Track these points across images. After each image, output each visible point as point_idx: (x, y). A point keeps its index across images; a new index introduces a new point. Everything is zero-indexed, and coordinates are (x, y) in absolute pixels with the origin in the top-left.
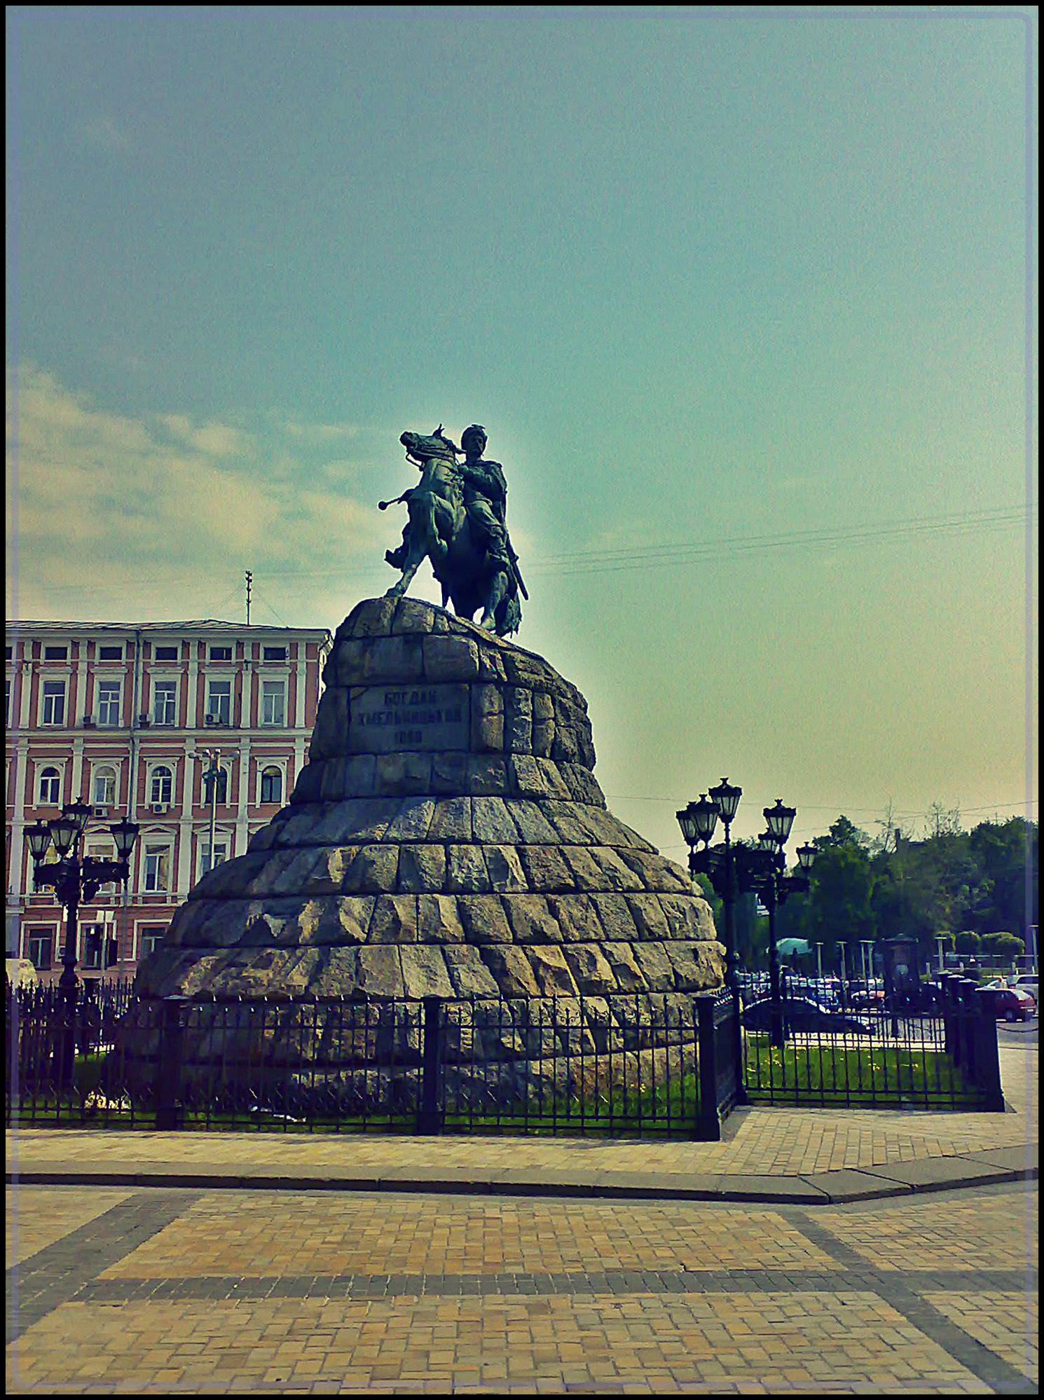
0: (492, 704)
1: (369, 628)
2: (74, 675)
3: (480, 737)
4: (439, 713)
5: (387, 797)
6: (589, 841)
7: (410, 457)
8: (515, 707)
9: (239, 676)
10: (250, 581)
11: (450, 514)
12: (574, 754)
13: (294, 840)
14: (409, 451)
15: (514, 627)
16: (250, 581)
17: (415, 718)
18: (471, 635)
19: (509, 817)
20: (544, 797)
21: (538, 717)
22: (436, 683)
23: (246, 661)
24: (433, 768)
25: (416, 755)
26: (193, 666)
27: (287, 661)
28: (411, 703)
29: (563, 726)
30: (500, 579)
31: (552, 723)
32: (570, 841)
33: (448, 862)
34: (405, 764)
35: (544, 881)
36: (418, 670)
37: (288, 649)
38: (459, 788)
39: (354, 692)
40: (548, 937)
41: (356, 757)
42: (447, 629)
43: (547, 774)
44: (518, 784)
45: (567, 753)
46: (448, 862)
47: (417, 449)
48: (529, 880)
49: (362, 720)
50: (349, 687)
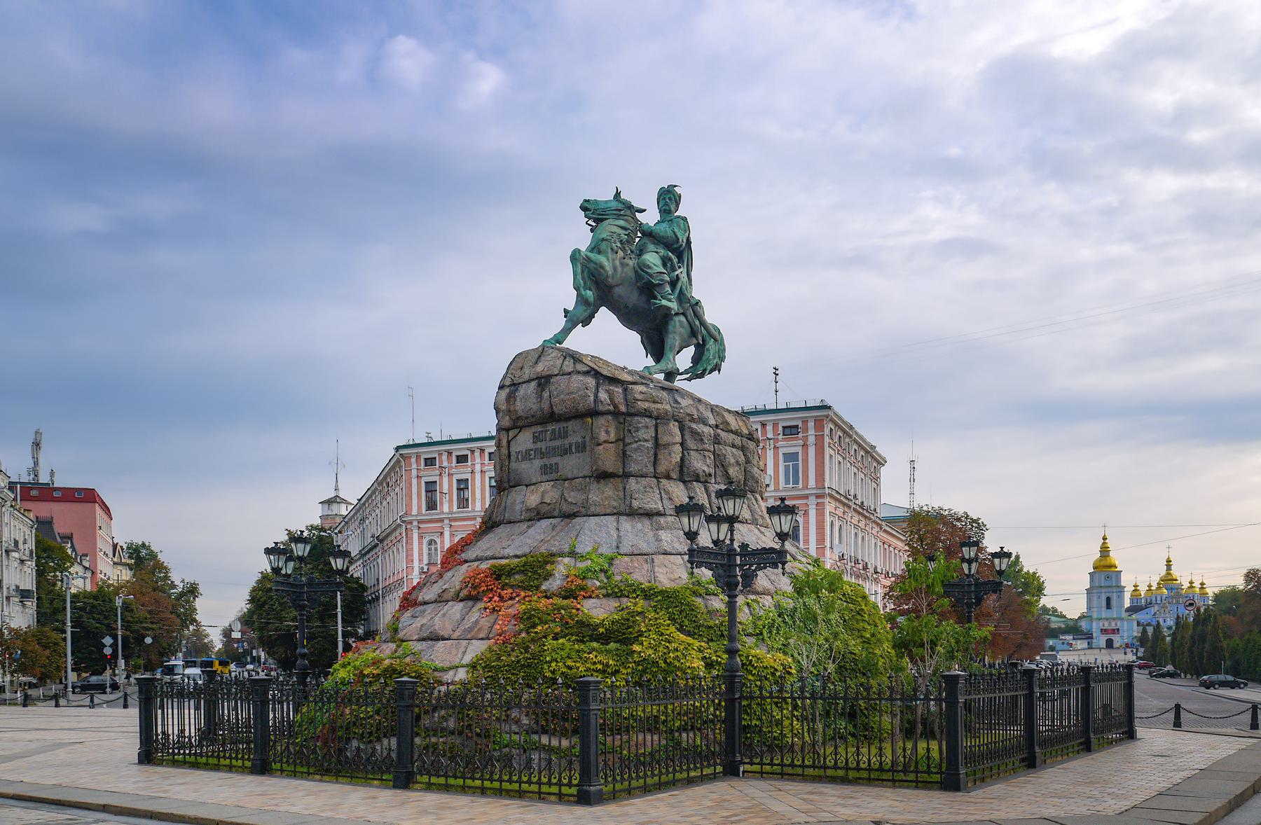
0: (607, 432)
3: (596, 462)
4: (570, 446)
5: (530, 520)
8: (634, 434)
17: (552, 452)
18: (593, 372)
20: (659, 514)
21: (660, 442)
22: (568, 419)
24: (563, 494)
25: (552, 483)
27: (800, 435)
29: (697, 450)
30: (678, 324)
31: (678, 448)
32: (666, 550)
36: (546, 406)
39: (511, 434)
41: (514, 489)
42: (571, 369)
43: (667, 492)
45: (698, 475)
49: (518, 458)
50: (507, 430)
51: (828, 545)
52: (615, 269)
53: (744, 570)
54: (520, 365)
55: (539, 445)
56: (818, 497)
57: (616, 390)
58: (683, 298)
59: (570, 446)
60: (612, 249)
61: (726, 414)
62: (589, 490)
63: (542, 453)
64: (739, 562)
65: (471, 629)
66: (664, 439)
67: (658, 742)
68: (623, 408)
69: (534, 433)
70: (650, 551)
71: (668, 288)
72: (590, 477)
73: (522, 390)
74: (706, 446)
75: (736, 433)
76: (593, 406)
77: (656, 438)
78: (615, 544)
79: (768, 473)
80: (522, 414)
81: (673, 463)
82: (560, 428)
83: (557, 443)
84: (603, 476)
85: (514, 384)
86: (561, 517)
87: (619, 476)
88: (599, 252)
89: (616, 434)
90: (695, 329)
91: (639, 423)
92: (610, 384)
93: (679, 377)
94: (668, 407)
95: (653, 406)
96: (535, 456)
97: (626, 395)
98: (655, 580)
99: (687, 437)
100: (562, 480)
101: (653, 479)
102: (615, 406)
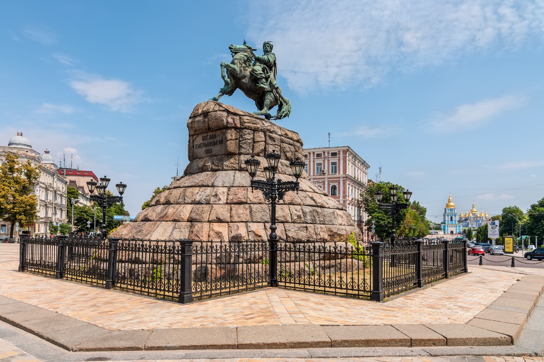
0: (231, 135)
4: (217, 141)
9: (324, 160)
17: (210, 144)
21: (255, 140)
23: (326, 157)
24: (213, 162)
26: (312, 159)
27: (337, 156)
29: (272, 145)
33: (198, 193)
34: (205, 161)
35: (232, 200)
37: (337, 152)
38: (220, 168)
40: (222, 220)
48: (227, 199)
51: (348, 195)
52: (241, 71)
56: (343, 178)
57: (236, 118)
58: (271, 84)
59: (217, 141)
60: (240, 63)
61: (286, 131)
65: (163, 217)
66: (257, 139)
67: (242, 270)
68: (239, 125)
71: (264, 80)
72: (224, 155)
74: (276, 143)
75: (291, 139)
76: (225, 124)
77: (254, 139)
78: (232, 182)
79: (326, 169)
81: (261, 149)
88: (234, 64)
89: (235, 136)
90: (277, 98)
91: (246, 132)
93: (271, 119)
94: (259, 126)
95: (252, 125)
97: (240, 120)
98: (247, 198)
99: (268, 139)
102: (235, 125)
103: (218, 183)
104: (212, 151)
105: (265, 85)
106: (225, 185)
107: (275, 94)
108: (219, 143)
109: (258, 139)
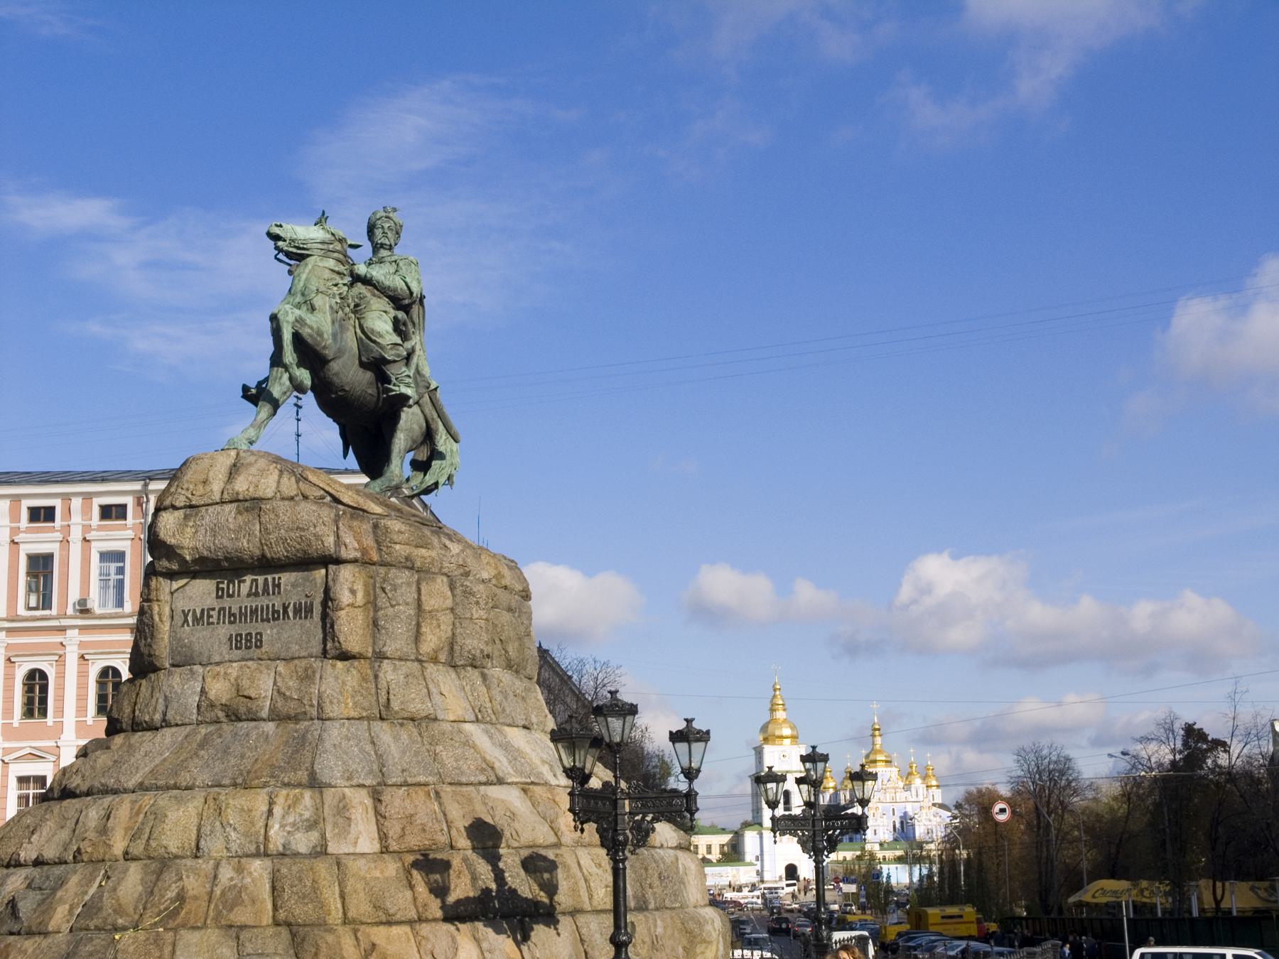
0: (353, 592)
1: (193, 494)
2: (65, 542)
4: (285, 608)
6: (483, 779)
7: (281, 256)
8: (390, 595)
10: (300, 407)
11: (320, 334)
12: (488, 656)
13: (84, 788)
14: (279, 250)
15: (442, 481)
16: (299, 407)
19: (369, 748)
24: (275, 683)
28: (249, 595)
44: (388, 699)
46: (270, 812)
47: (287, 246)
48: (383, 837)
49: (186, 621)
53: (635, 822)
54: (203, 477)
55: (227, 602)
59: (285, 608)
62: (321, 678)
63: (231, 615)
64: (627, 809)
66: (430, 603)
69: (218, 583)
70: (431, 779)
73: (209, 515)
80: (206, 553)
82: (266, 580)
83: (262, 601)
84: (345, 656)
85: (191, 507)
86: (273, 720)
87: (365, 658)
89: (367, 593)
92: (352, 517)
94: (434, 554)
96: (219, 619)
98: (449, 827)
100: (269, 659)
101: (416, 664)
102: (364, 551)
103: (330, 766)
104: (261, 642)
105: (408, 385)
106: (355, 782)
107: (427, 411)
108: (297, 611)
109: (432, 602)
